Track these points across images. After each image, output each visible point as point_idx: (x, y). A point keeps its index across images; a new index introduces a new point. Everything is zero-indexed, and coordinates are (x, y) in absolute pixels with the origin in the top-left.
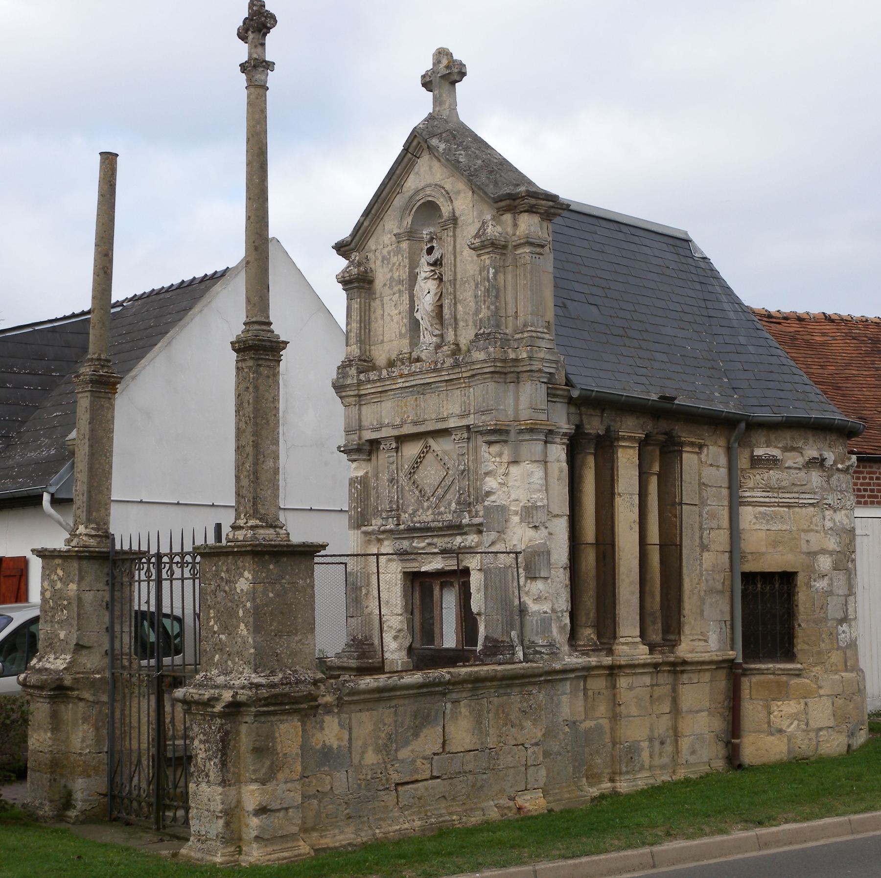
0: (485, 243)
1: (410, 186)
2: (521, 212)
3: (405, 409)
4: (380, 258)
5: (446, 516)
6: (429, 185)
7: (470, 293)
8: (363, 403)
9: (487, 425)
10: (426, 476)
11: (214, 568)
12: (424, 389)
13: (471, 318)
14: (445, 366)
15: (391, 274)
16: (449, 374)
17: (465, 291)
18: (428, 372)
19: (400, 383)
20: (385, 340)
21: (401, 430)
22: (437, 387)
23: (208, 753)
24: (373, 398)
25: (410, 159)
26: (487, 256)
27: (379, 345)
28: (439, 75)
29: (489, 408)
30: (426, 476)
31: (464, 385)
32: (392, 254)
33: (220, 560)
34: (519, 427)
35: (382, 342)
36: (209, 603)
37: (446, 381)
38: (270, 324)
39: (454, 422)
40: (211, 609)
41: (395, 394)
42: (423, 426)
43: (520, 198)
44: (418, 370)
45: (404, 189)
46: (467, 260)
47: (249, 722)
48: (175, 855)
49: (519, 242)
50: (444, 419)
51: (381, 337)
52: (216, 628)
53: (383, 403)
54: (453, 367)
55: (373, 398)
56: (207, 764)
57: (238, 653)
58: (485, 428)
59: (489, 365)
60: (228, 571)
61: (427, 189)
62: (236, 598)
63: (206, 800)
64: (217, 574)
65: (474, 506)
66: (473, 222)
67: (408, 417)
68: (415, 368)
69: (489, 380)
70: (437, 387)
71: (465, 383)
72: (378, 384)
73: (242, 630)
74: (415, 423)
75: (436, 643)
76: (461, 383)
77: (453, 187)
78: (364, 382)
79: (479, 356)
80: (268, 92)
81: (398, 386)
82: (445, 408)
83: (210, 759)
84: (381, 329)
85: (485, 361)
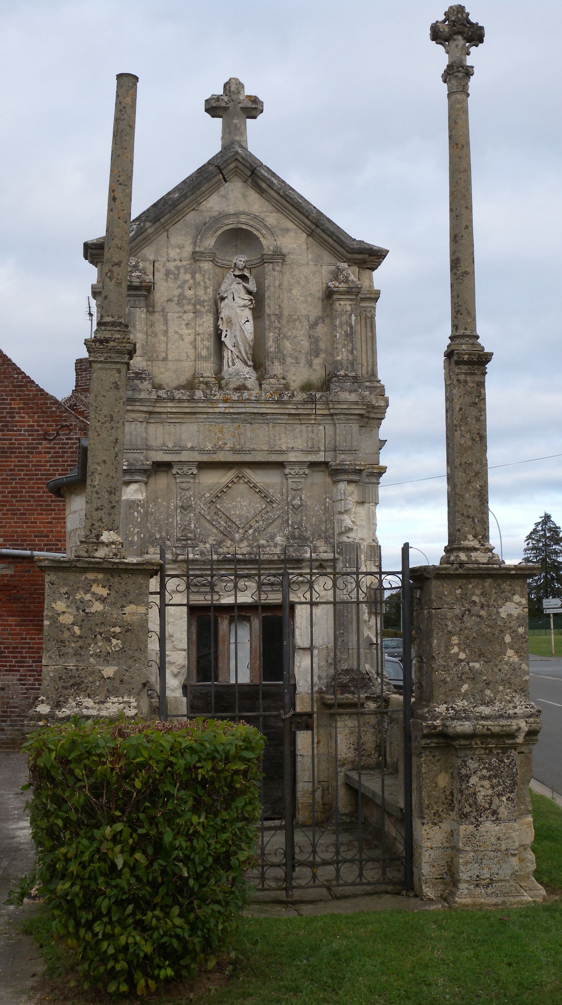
0: (354, 290)
1: (212, 208)
2: (366, 268)
3: (219, 435)
4: (163, 271)
5: (270, 550)
6: (244, 213)
7: (302, 332)
8: (152, 421)
9: (356, 465)
10: (235, 507)
11: (458, 592)
12: (252, 419)
13: (303, 356)
14: (295, 399)
15: (180, 291)
16: (297, 408)
17: (294, 328)
18: (267, 402)
19: (222, 407)
20: (170, 357)
21: (214, 456)
22: (275, 419)
23: (496, 789)
24: (171, 418)
25: (220, 180)
26: (348, 303)
27: (160, 364)
28: (240, 105)
29: (354, 449)
30: (235, 507)
31: (313, 422)
32: (182, 270)
33: (470, 583)
34: (370, 470)
35: (165, 359)
36: (449, 628)
37: (289, 414)
38: (477, 337)
39: (296, 456)
40: (454, 635)
41: (209, 418)
42: (250, 456)
43: (378, 256)
44: (253, 398)
45: (202, 207)
46: (298, 299)
47: (526, 751)
48: (67, 945)
49: (368, 296)
50: (282, 452)
51: (164, 355)
52: (462, 656)
53: (182, 425)
54: (305, 402)
55: (171, 418)
56: (496, 801)
57: (502, 681)
58: (352, 467)
59: (360, 407)
60: (484, 594)
61: (243, 216)
62: (499, 623)
63: (493, 840)
64: (464, 597)
65: (312, 542)
66: (308, 264)
67: (226, 444)
68: (249, 395)
69: (354, 421)
70: (275, 419)
71: (315, 420)
72: (186, 404)
73: (509, 657)
74: (234, 451)
75: (220, 679)
76: (311, 419)
77: (279, 223)
78: (164, 399)
79: (348, 397)
80: (469, 99)
81: (217, 410)
82: (283, 441)
83: (499, 795)
84: (163, 345)
85: (357, 403)
